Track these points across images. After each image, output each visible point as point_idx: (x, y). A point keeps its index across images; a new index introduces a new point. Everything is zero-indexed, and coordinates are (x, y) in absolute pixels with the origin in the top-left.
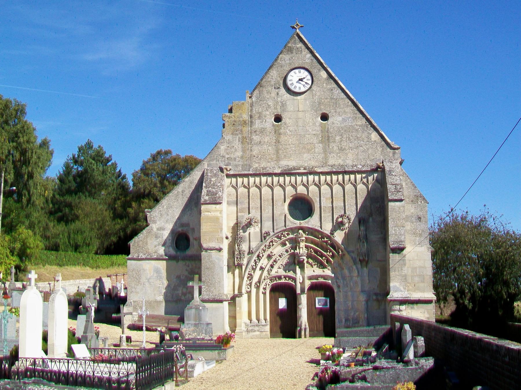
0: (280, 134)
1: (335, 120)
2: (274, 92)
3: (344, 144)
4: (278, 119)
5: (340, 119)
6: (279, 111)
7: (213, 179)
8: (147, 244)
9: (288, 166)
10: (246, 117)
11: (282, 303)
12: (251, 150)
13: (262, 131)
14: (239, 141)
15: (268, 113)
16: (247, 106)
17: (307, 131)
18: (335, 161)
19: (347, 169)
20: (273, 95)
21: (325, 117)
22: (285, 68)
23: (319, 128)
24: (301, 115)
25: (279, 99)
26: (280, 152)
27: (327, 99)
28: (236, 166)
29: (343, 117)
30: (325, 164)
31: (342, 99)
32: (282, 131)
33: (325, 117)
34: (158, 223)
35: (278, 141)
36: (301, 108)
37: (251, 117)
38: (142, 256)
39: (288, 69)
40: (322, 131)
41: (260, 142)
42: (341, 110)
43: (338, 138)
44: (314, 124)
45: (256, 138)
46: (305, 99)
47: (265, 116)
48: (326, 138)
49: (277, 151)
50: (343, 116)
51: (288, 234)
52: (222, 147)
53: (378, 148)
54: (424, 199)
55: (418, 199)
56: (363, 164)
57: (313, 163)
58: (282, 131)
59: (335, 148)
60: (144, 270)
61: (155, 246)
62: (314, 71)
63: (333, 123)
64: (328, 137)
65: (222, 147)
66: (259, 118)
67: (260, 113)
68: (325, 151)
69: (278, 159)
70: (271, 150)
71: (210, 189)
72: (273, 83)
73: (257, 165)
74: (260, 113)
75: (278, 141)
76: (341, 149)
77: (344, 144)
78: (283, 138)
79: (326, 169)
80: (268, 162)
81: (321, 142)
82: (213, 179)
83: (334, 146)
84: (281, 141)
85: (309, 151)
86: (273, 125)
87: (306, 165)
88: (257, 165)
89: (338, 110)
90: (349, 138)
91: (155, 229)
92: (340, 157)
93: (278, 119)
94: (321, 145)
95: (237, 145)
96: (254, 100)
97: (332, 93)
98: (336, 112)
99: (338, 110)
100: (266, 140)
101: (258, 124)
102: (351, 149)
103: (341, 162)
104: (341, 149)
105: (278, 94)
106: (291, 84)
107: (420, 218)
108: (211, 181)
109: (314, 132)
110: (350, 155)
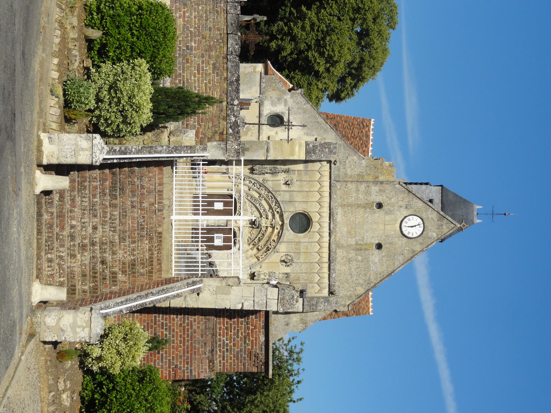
0: (365, 208)
1: (376, 256)
2: (403, 204)
3: (354, 263)
4: (380, 206)
5: (377, 260)
6: (385, 207)
7: (327, 149)
8: (273, 90)
9: (337, 214)
10: (381, 178)
11: (219, 206)
12: (352, 182)
13: (368, 193)
14: (360, 172)
15: (384, 198)
16: (392, 179)
17: (367, 232)
18: (340, 254)
19: (332, 264)
20: (400, 203)
21: (379, 246)
22: (424, 214)
23: (369, 241)
24: (381, 227)
25: (396, 208)
26: (350, 208)
27: (395, 249)
28: (339, 170)
29: (378, 263)
30: (338, 246)
31: (394, 263)
32: (368, 210)
33: (379, 246)
34: (291, 100)
35: (359, 206)
36: (388, 227)
37: (382, 183)
38: (263, 85)
39: (424, 217)
40: (365, 245)
41: (359, 191)
42: (384, 261)
43: (360, 258)
44: (373, 237)
45: (363, 187)
46: (395, 230)
47: (381, 195)
48: (360, 248)
49: (350, 205)
50: (378, 264)
51: (278, 212)
52: (355, 157)
53: (350, 292)
54: (304, 329)
55: (304, 323)
56: (336, 278)
57: (338, 235)
58: (368, 210)
59: (351, 256)
60: (251, 88)
61: (271, 98)
62: (420, 240)
63: (373, 254)
64: (361, 250)
65: (355, 157)
66: (380, 190)
67: (384, 191)
68: (349, 246)
69: (343, 206)
70: (352, 200)
71: (319, 148)
72: (411, 203)
73: (338, 187)
74: (384, 191)
75: (359, 206)
76: (350, 260)
77: (354, 263)
78: (361, 211)
79: (333, 246)
80: (341, 197)
81: (357, 244)
82: (327, 149)
83: (352, 254)
84: (359, 208)
85: (349, 232)
86: (373, 202)
87: (337, 230)
88: (338, 187)
89: (384, 259)
90: (359, 268)
91: (285, 97)
92: (342, 259)
93: (380, 206)
94: (354, 243)
95: (357, 171)
96: (397, 186)
97: (400, 255)
98: (383, 257)
99: (384, 259)
100: (360, 196)
101: (374, 189)
102: (350, 269)
103: (339, 259)
104: (350, 260)
105: (401, 207)
106: (409, 219)
107: (287, 324)
108: (325, 148)
109: (365, 237)
110: (343, 268)
